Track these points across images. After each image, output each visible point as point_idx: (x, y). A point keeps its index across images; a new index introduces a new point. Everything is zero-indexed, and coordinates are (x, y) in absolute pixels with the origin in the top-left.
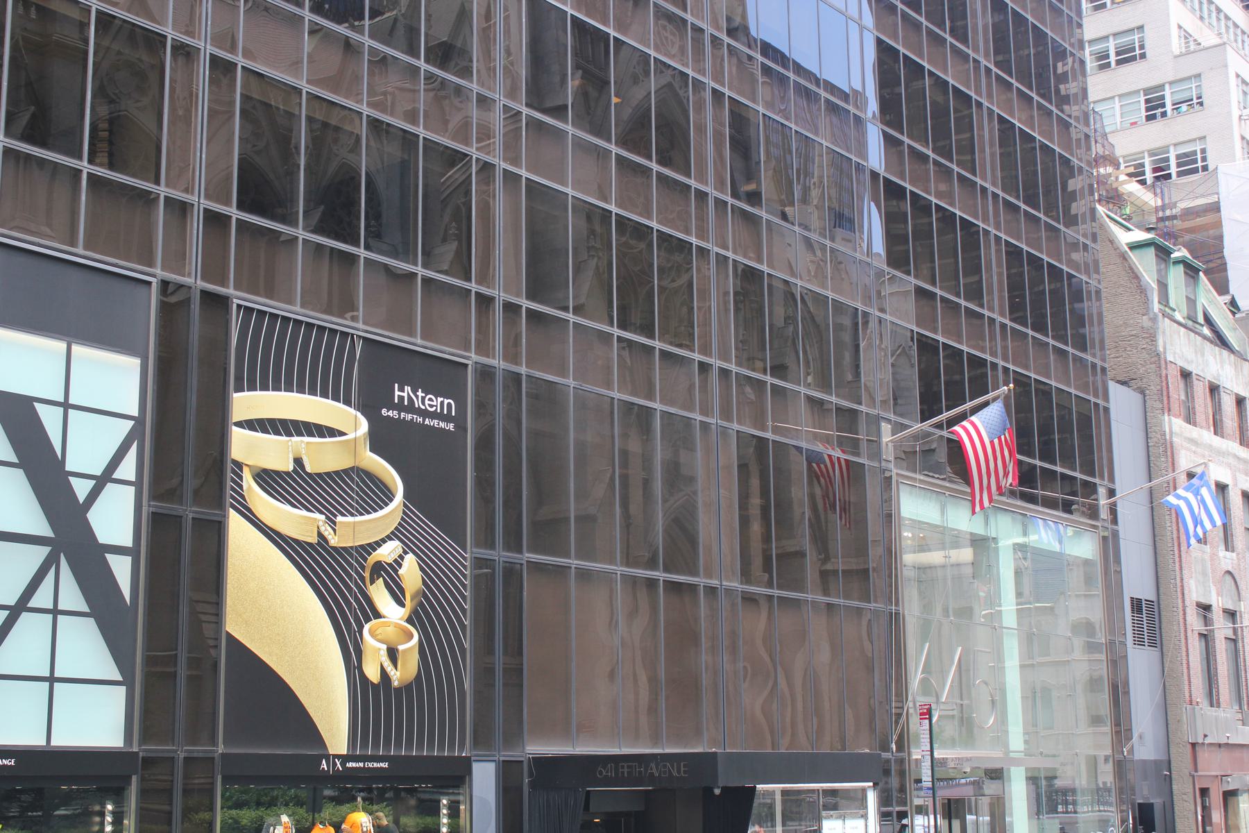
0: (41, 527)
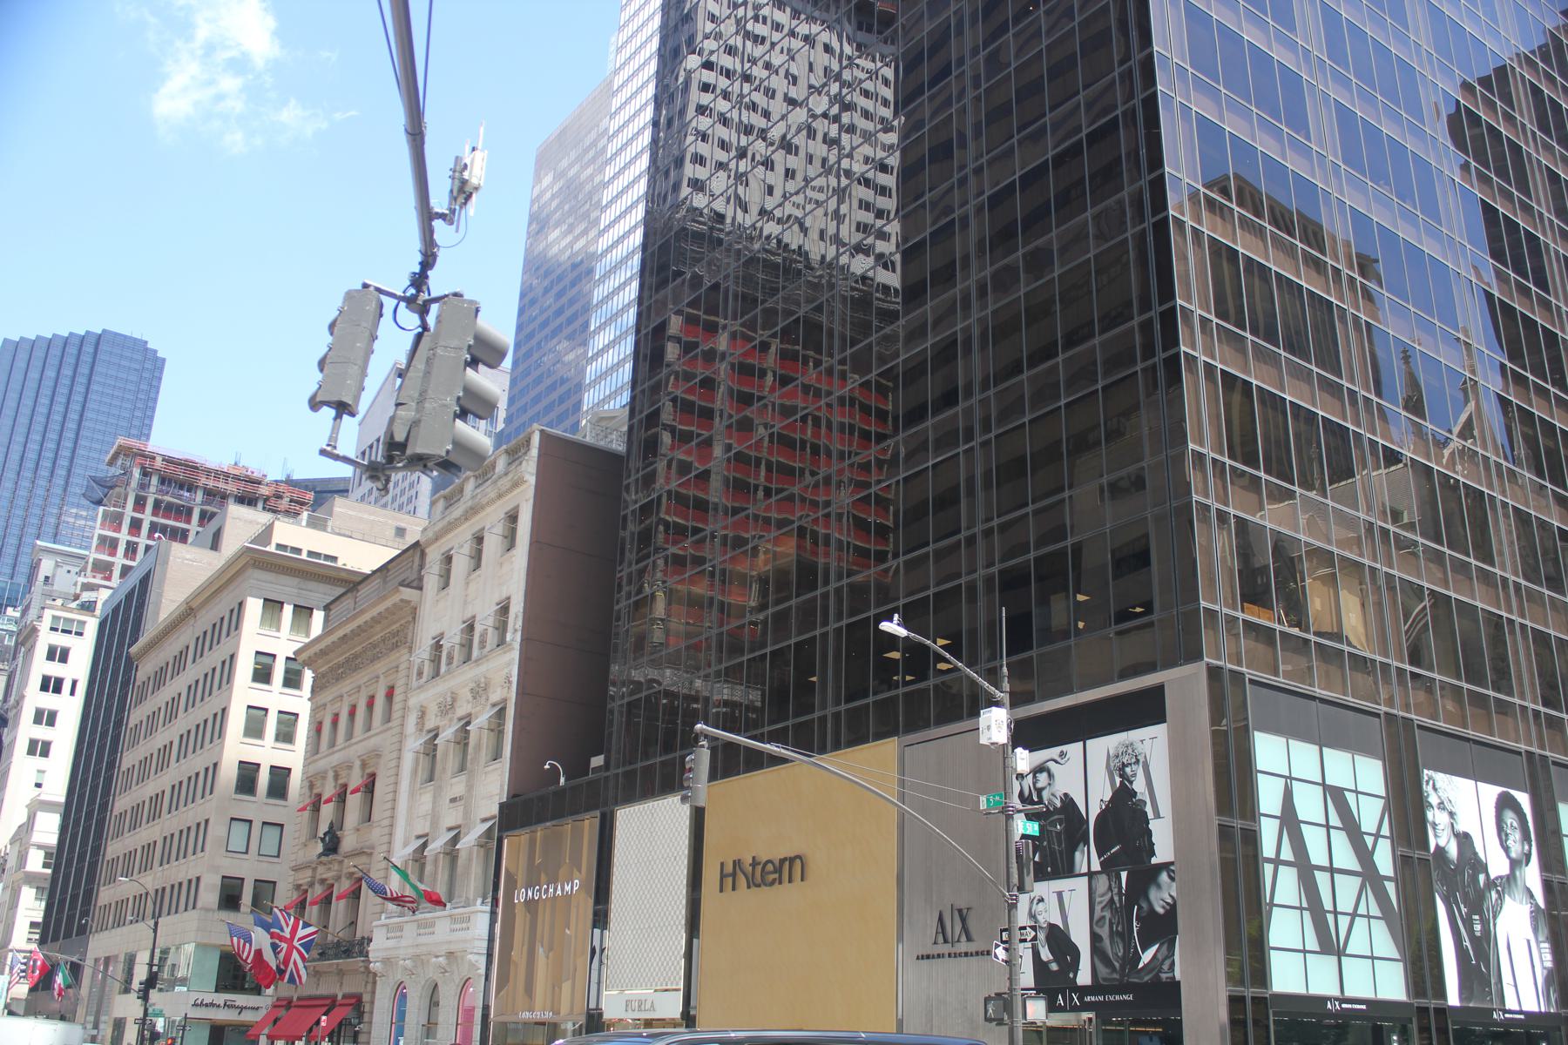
0: (1356, 867)
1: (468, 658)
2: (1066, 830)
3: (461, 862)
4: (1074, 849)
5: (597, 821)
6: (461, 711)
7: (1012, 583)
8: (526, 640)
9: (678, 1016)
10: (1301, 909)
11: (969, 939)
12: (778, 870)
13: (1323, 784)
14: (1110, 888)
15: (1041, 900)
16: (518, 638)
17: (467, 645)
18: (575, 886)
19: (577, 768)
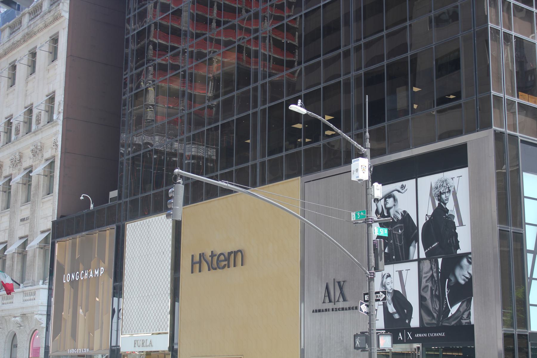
1: (29, 131)
3: (29, 258)
4: (410, 246)
5: (114, 231)
6: (26, 163)
7: (372, 80)
8: (66, 119)
9: (167, 349)
11: (345, 300)
12: (227, 259)
14: (431, 269)
15: (389, 276)
16: (61, 117)
17: (28, 123)
18: (102, 271)
19: (101, 198)
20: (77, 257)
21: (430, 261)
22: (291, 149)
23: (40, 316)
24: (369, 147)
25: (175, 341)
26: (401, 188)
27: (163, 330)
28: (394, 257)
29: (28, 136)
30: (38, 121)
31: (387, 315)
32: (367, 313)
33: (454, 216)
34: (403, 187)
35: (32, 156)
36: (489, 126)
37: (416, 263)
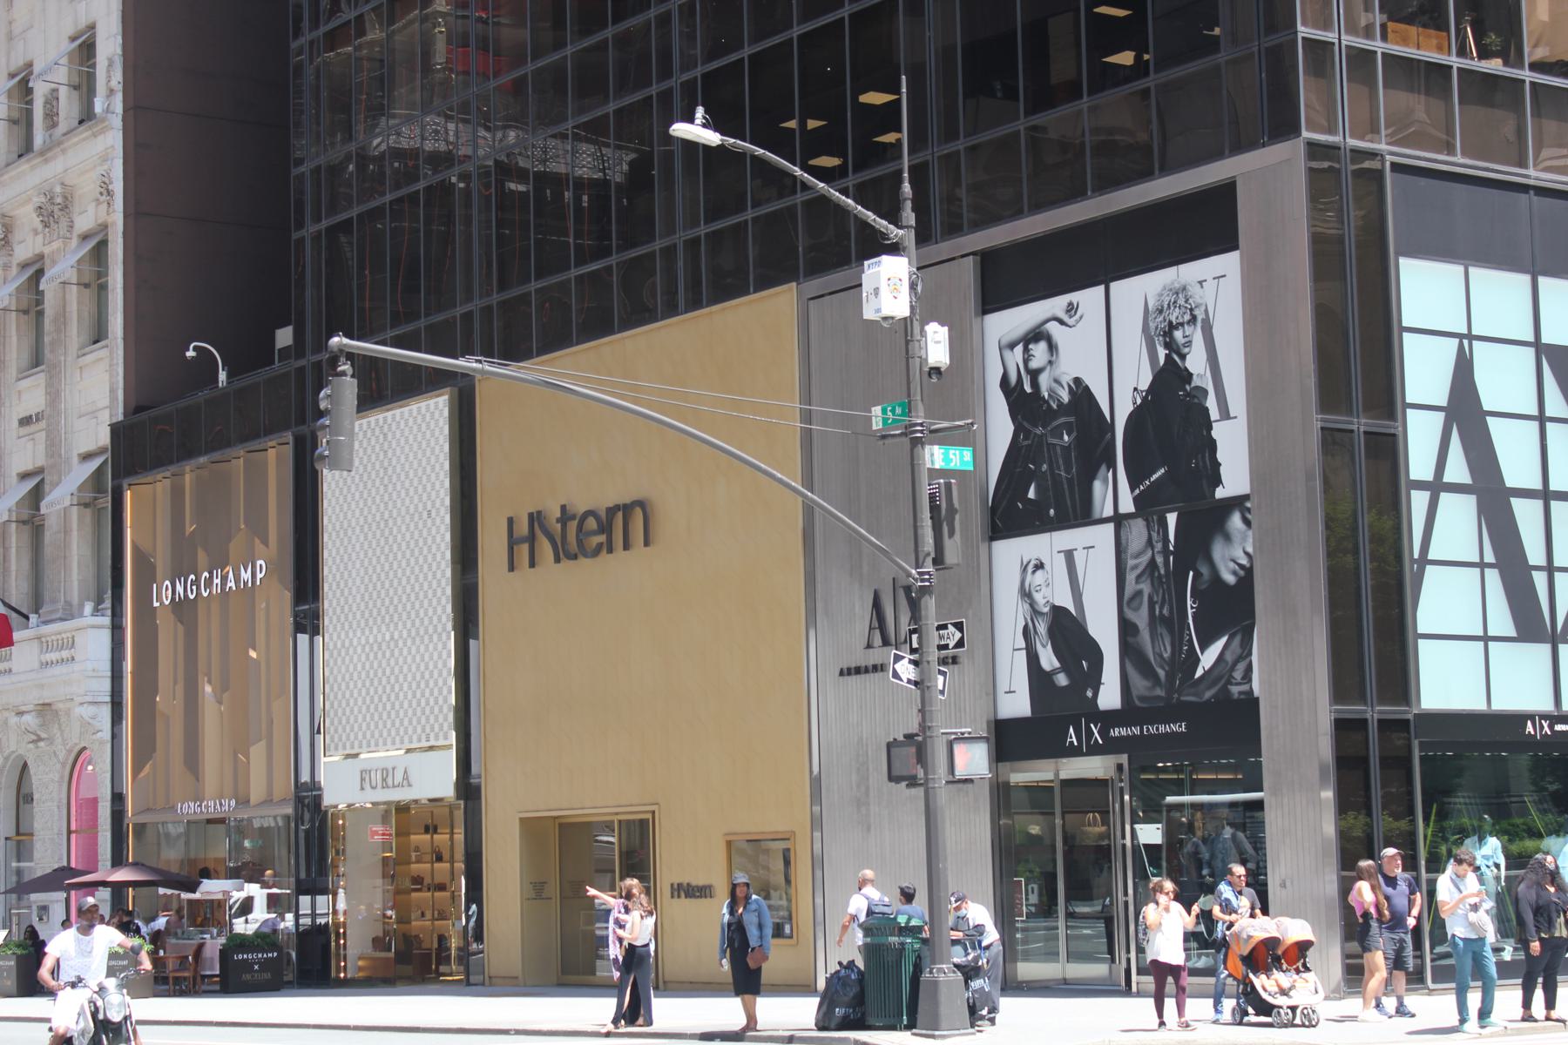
1: (25, 149)
2: (1079, 442)
5: (289, 450)
8: (134, 110)
10: (1482, 565)
12: (605, 528)
13: (1537, 345)
14: (1150, 543)
15: (1040, 566)
16: (118, 106)
18: (257, 571)
19: (250, 353)
20: (190, 528)
21: (1146, 520)
22: (768, 200)
23: (92, 710)
24: (913, 223)
25: (474, 770)
26: (1068, 311)
27: (437, 738)
28: (1052, 512)
29: (23, 166)
30: (51, 117)
31: (1038, 678)
32: (916, 683)
33: (1205, 392)
34: (1071, 309)
35: (40, 227)
36: (1294, 130)
37: (1110, 527)
